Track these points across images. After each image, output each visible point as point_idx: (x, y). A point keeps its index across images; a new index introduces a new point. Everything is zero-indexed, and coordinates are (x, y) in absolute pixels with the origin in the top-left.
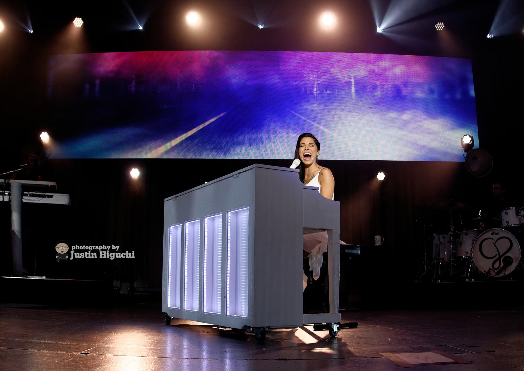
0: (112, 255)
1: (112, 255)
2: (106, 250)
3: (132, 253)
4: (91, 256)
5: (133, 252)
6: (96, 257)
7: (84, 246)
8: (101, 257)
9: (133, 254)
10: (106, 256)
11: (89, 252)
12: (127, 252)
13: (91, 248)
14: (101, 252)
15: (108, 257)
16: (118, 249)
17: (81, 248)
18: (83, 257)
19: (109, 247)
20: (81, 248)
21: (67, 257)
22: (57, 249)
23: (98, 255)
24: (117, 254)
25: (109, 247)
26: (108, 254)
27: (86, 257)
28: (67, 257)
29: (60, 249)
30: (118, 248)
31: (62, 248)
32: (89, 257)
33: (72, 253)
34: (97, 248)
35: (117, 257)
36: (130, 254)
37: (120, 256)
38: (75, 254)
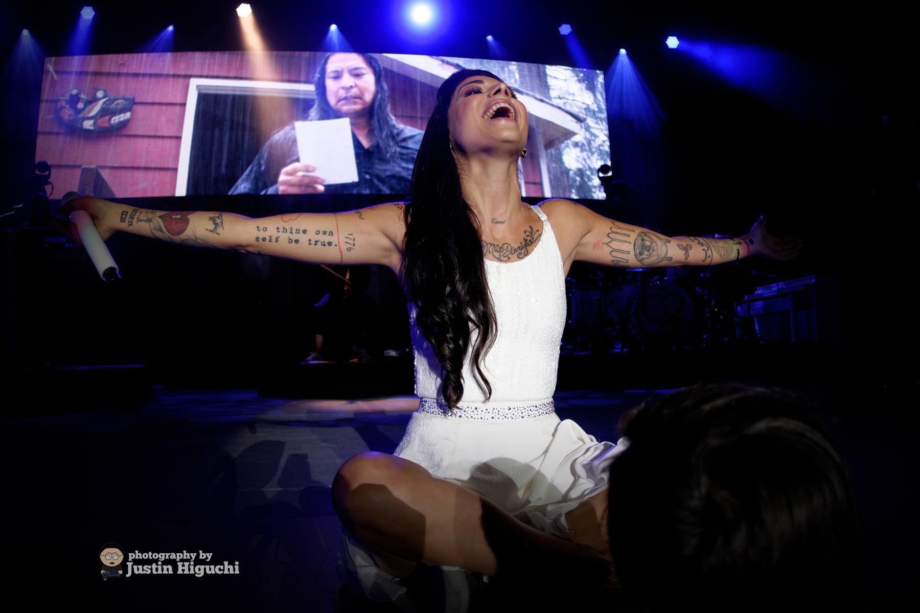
7: (150, 553)
13: (162, 556)
16: (209, 558)
17: (145, 556)
19: (194, 556)
20: (145, 556)
25: (194, 556)
29: (108, 558)
30: (209, 556)
31: (111, 557)
34: (173, 556)
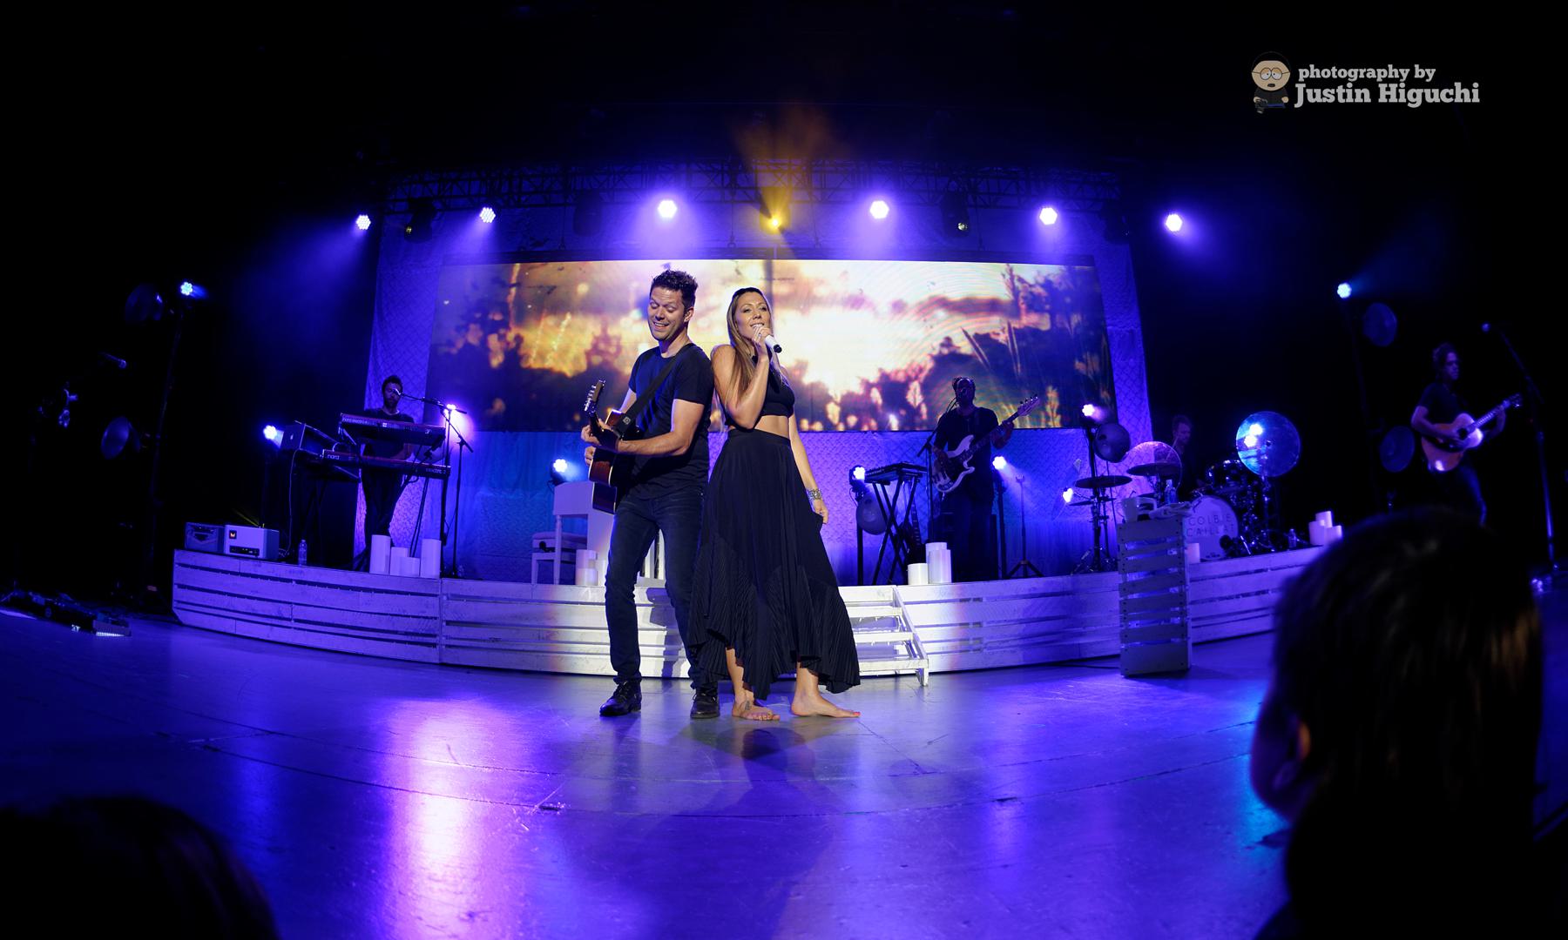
4: (1354, 96)
6: (1368, 99)
8: (1382, 99)
9: (1476, 92)
10: (1398, 96)
15: (1403, 100)
18: (1332, 99)
21: (1286, 100)
23: (1375, 94)
24: (1427, 91)
26: (1402, 92)
27: (1341, 100)
28: (1286, 100)
32: (1350, 99)
35: (1429, 100)
36: (1466, 91)
37: (1438, 96)
38: (1309, 91)
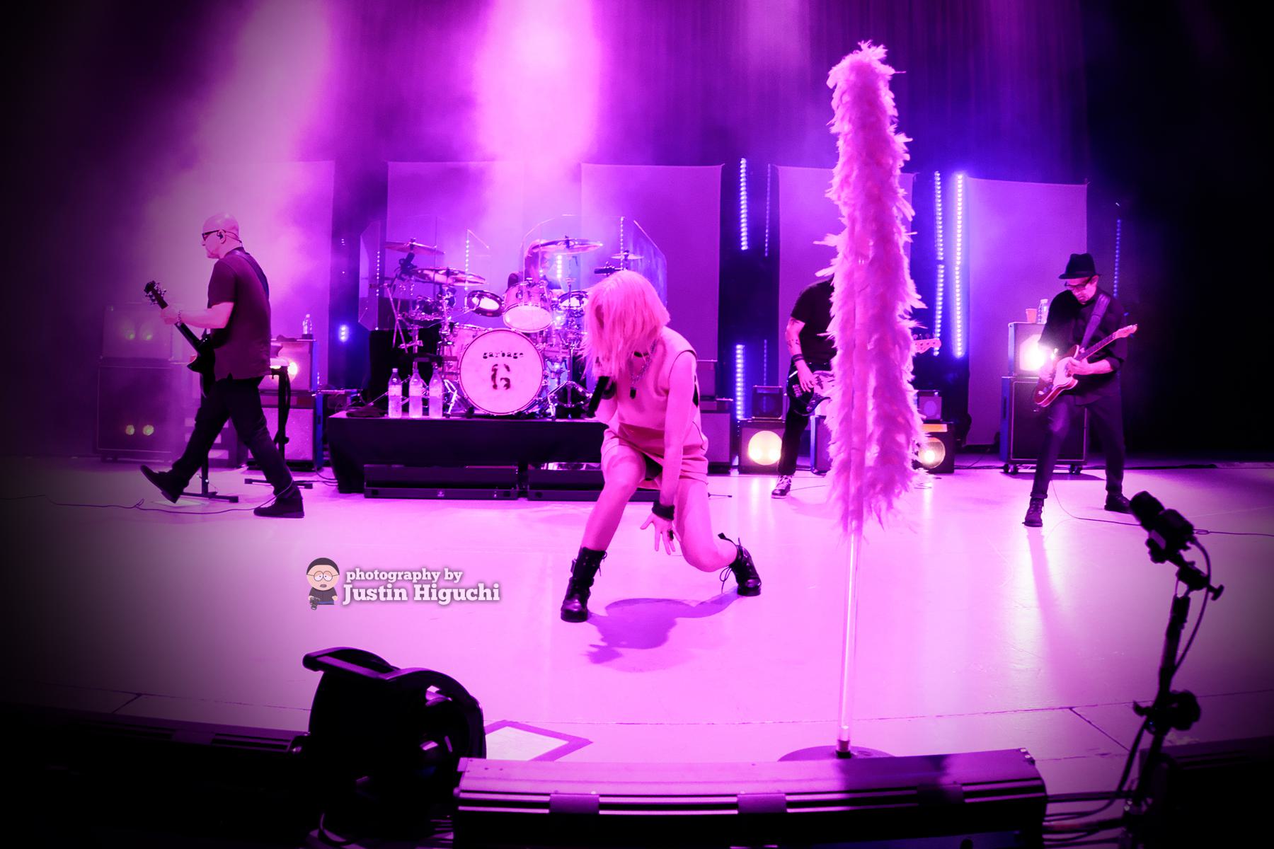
0: (444, 594)
1: (444, 594)
2: (430, 582)
3: (492, 589)
4: (393, 595)
5: (496, 586)
7: (376, 573)
10: (430, 595)
11: (390, 586)
12: (481, 586)
14: (418, 587)
16: (458, 578)
22: (309, 578)
23: (411, 594)
26: (434, 592)
27: (382, 598)
29: (318, 578)
33: (348, 587)
34: (408, 576)
36: (488, 591)
